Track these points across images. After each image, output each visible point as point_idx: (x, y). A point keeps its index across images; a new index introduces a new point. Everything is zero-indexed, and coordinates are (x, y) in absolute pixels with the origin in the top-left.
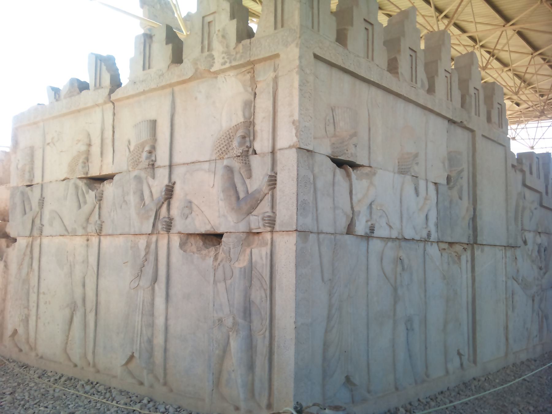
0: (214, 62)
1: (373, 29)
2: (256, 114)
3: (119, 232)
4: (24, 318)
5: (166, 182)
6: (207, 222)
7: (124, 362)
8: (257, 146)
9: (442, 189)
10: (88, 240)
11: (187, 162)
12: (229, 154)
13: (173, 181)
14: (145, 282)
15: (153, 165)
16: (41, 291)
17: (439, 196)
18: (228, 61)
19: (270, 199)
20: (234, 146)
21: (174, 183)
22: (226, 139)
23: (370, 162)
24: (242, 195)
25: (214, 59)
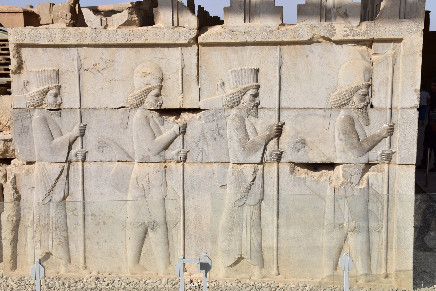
0: (335, 33)
4: (62, 241)
6: (322, 154)
10: (166, 167)
11: (298, 107)
12: (347, 106)
13: (282, 121)
14: (252, 200)
15: (257, 107)
16: (88, 212)
18: (351, 35)
20: (355, 101)
22: (347, 95)
24: (361, 138)
25: (335, 30)
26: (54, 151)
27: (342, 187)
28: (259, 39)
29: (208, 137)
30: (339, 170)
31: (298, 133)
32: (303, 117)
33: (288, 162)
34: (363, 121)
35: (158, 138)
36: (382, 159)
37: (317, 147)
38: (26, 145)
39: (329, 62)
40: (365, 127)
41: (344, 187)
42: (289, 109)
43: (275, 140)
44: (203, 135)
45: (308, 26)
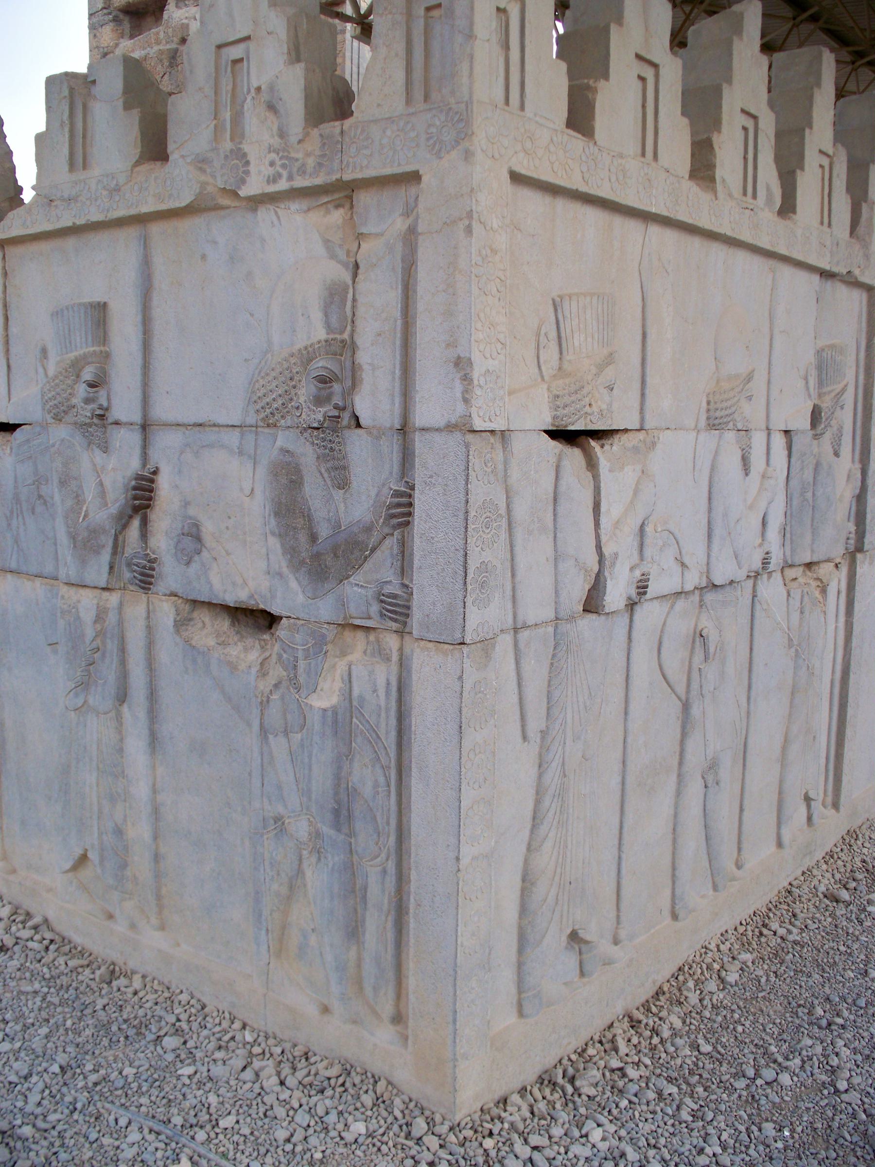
0: (247, 173)
1: (657, 76)
2: (358, 322)
3: (33, 570)
5: (135, 464)
7: (68, 865)
8: (363, 406)
9: (801, 442)
11: (186, 421)
15: (101, 417)
17: (793, 460)
18: (285, 174)
19: (396, 550)
20: (302, 400)
21: (155, 473)
23: (642, 420)
25: (248, 163)
27: (274, 697)
28: (96, 216)
29: (25, 506)
33: (168, 592)
34: (327, 470)
36: (382, 615)
37: (228, 554)
40: (338, 495)
41: (282, 698)
43: (136, 523)
44: (17, 498)
45: (189, 160)
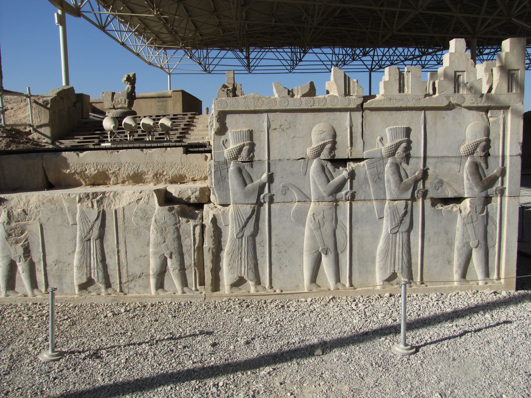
25: (464, 99)
26: (247, 195)
30: (467, 203)
31: (437, 175)
32: (441, 164)
35: (332, 182)
38: (223, 191)
39: (459, 123)
42: (431, 157)
